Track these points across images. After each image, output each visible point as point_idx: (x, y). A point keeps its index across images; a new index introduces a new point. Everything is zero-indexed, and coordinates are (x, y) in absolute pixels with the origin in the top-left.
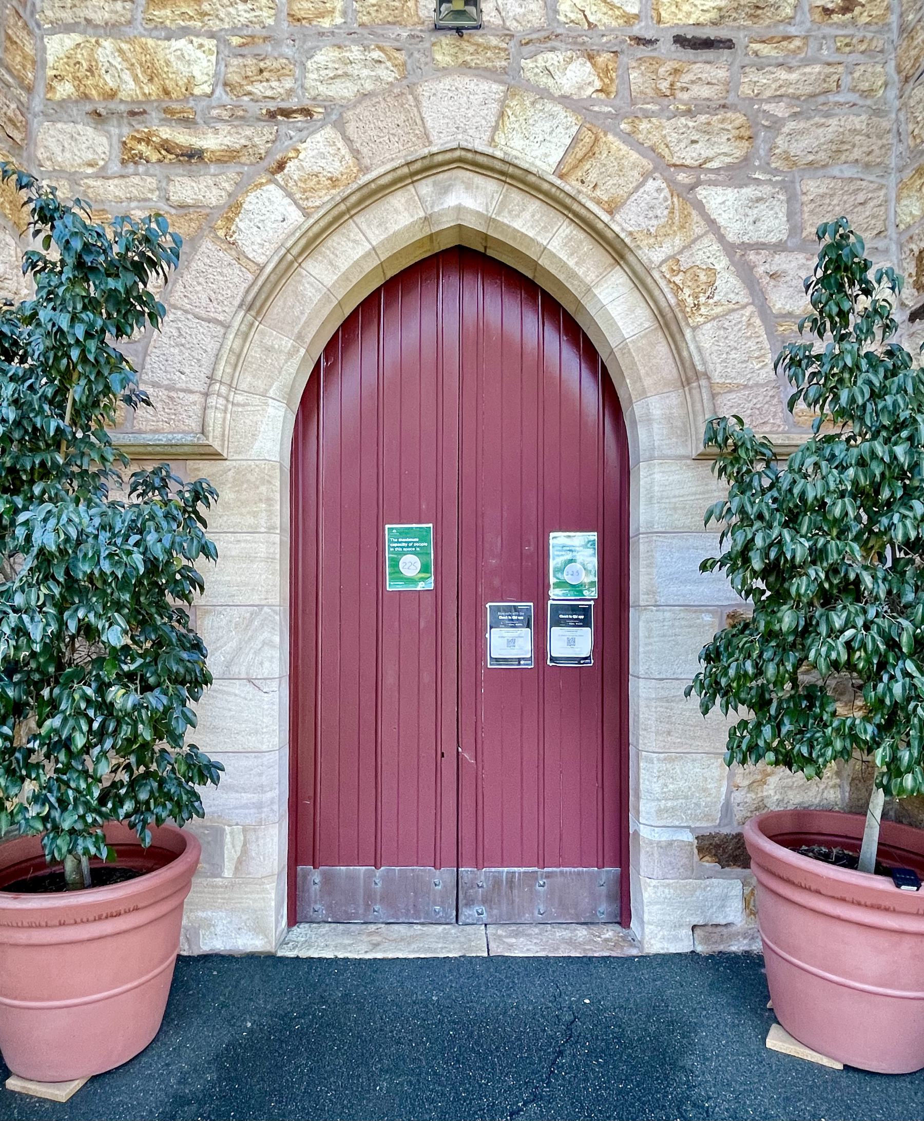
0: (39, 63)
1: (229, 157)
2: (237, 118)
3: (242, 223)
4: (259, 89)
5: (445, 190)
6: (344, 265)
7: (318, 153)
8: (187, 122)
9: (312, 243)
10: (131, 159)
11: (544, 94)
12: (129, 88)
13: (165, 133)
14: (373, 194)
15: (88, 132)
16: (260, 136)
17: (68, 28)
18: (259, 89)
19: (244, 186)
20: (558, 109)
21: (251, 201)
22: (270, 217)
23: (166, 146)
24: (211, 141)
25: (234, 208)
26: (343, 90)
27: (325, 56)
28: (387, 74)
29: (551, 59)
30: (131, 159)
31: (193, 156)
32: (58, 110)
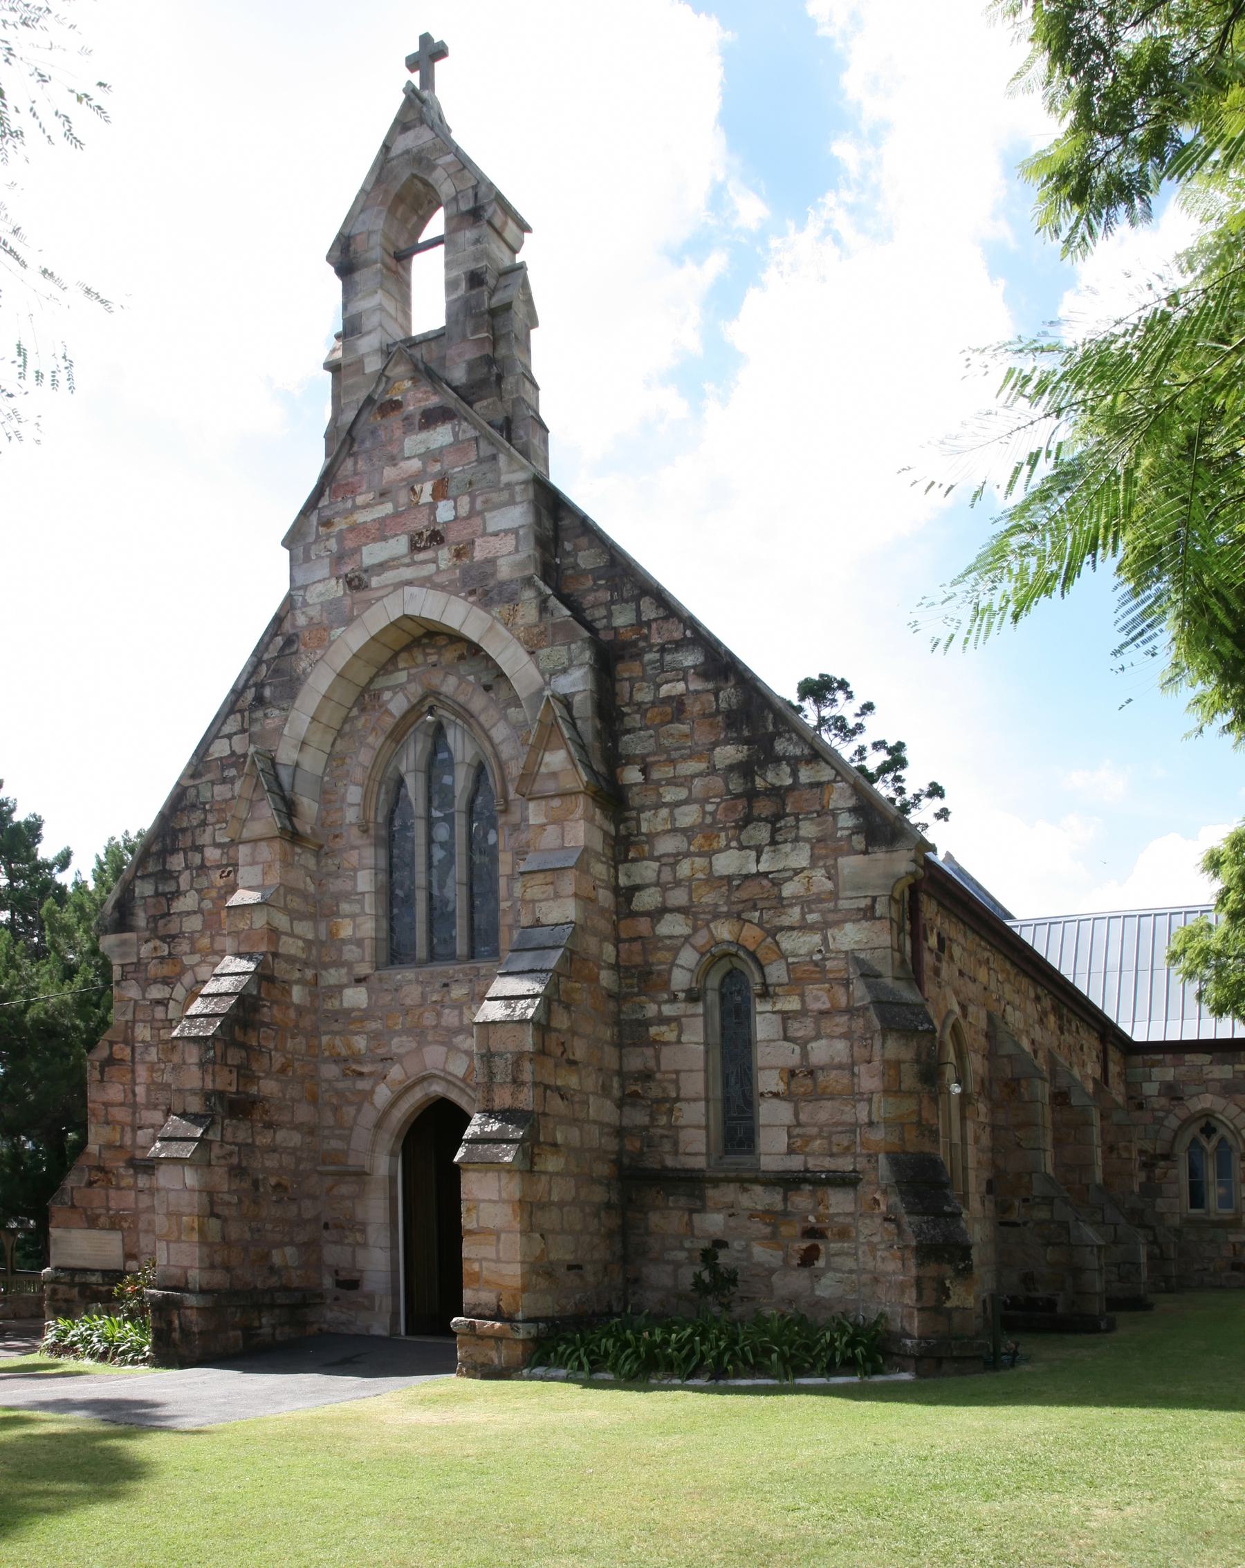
0: (320, 1045)
1: (371, 1074)
2: (373, 1062)
3: (375, 1097)
4: (379, 1051)
5: (430, 1085)
6: (403, 1110)
7: (396, 1072)
8: (359, 1062)
9: (393, 1104)
10: (345, 1075)
11: (458, 1050)
12: (344, 1052)
13: (354, 1067)
14: (409, 1089)
15: (333, 1067)
16: (379, 1067)
17: (326, 1033)
18: (379, 1051)
19: (376, 1084)
20: (463, 1056)
21: (378, 1089)
22: (383, 1094)
23: (354, 1071)
24: (365, 1069)
25: (372, 1092)
26: (402, 1051)
27: (395, 1041)
28: (414, 1045)
29: (461, 1037)
30: (345, 1075)
31: (361, 1074)
32: (326, 1060)
